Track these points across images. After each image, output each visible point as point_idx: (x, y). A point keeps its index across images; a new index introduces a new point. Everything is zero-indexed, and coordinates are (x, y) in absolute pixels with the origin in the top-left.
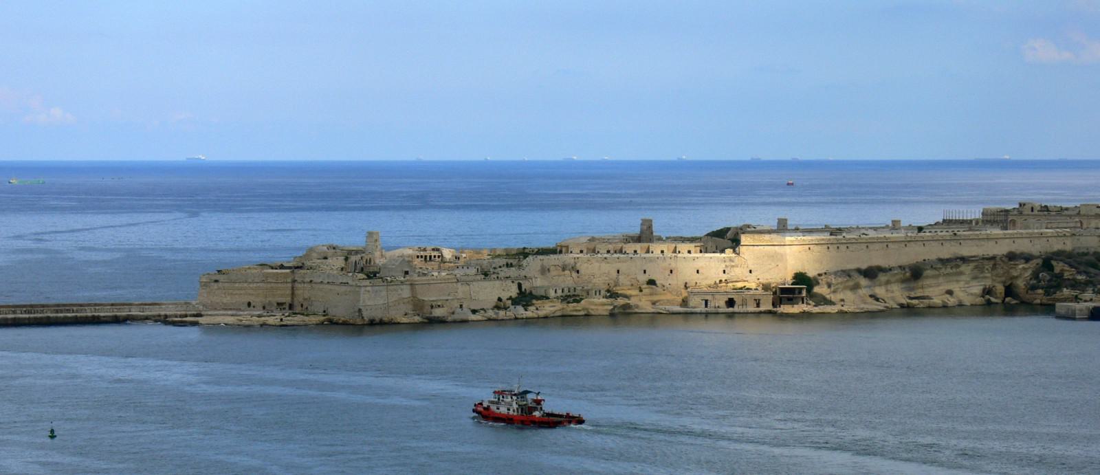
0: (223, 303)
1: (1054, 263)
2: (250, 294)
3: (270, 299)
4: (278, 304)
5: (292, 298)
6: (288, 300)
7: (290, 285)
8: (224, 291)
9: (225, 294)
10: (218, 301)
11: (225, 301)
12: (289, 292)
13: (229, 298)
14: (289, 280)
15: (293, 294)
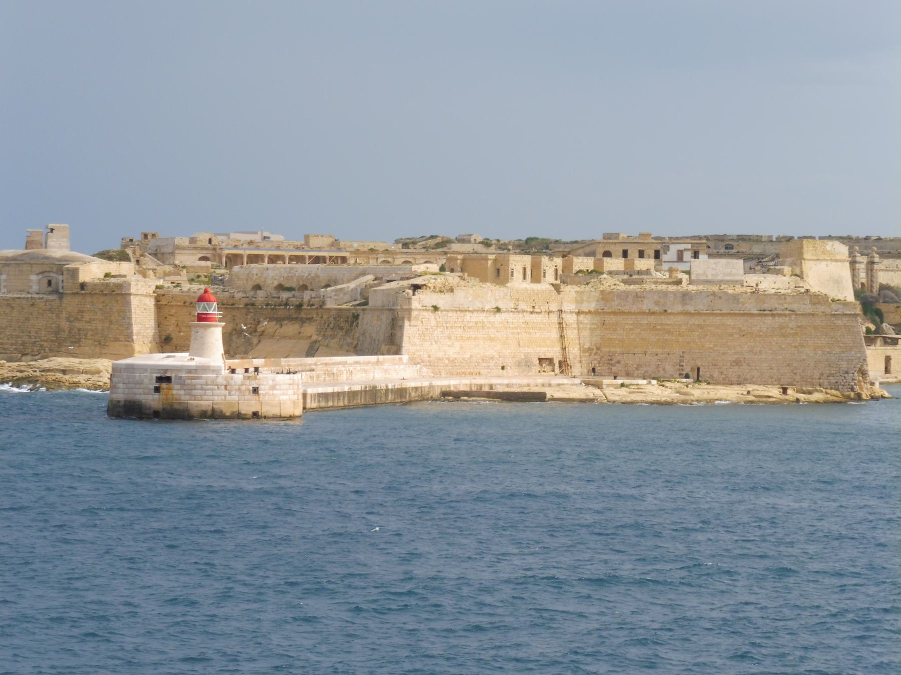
0: (448, 359)
1: (882, 307)
2: (491, 339)
3: (527, 350)
4: (541, 360)
5: (564, 349)
6: (554, 353)
7: (554, 318)
8: (447, 332)
9: (449, 338)
10: (440, 355)
11: (452, 353)
12: (555, 334)
13: (457, 345)
14: (554, 307)
15: (562, 337)
